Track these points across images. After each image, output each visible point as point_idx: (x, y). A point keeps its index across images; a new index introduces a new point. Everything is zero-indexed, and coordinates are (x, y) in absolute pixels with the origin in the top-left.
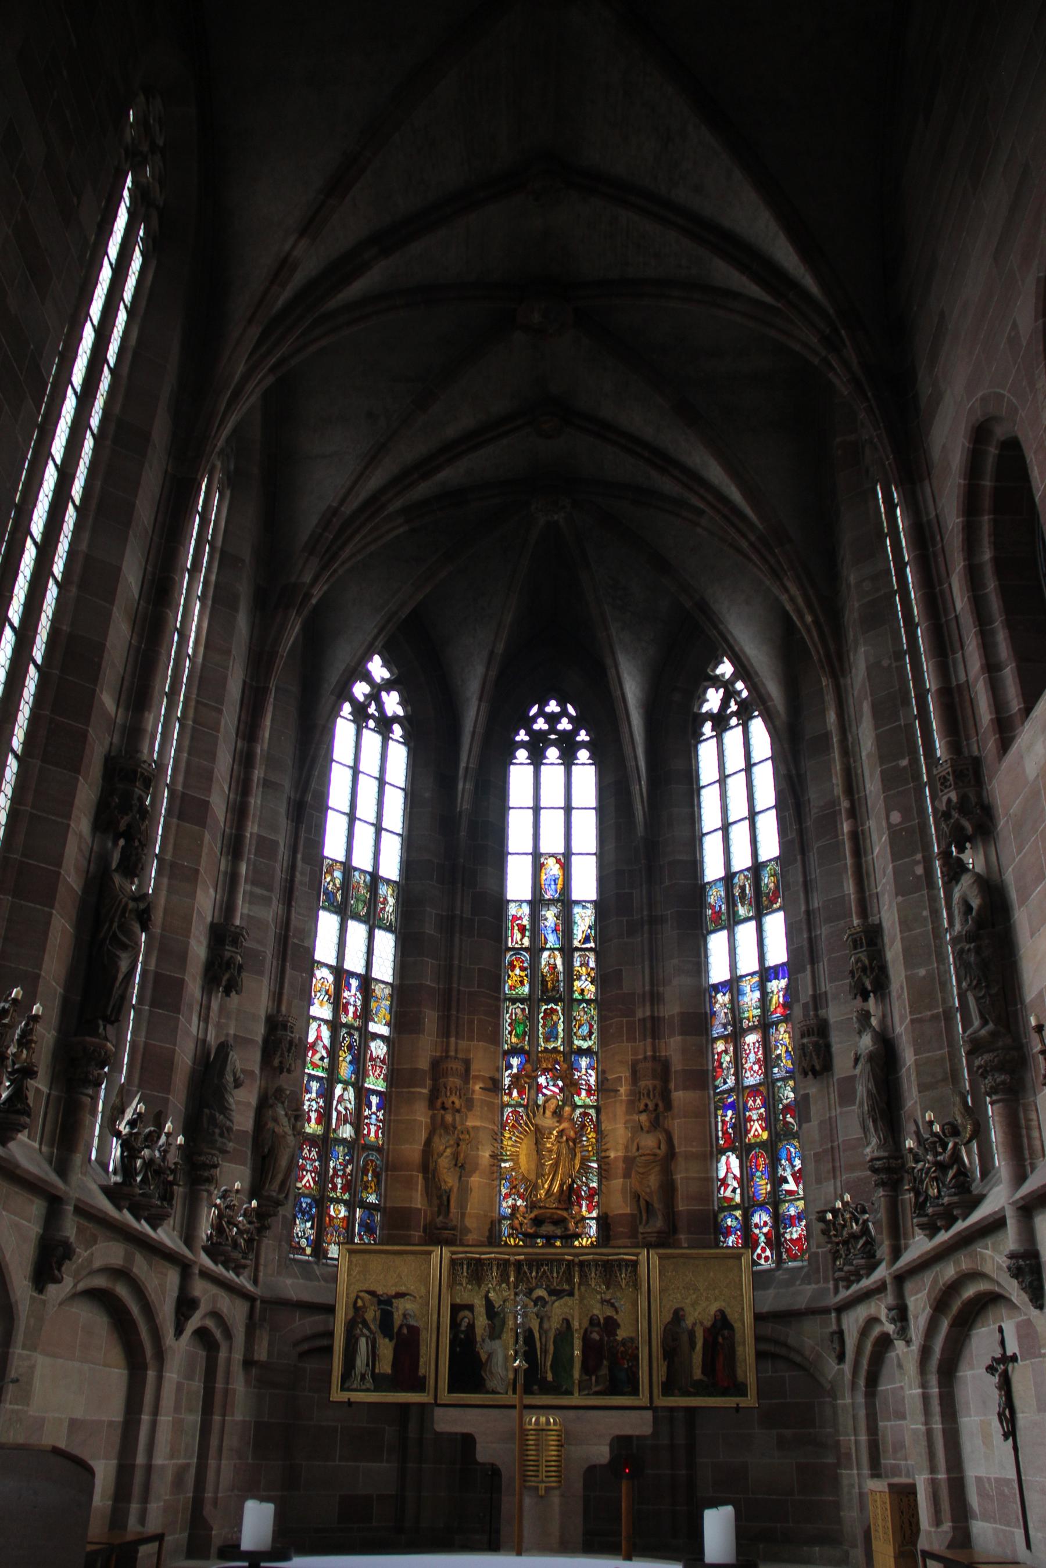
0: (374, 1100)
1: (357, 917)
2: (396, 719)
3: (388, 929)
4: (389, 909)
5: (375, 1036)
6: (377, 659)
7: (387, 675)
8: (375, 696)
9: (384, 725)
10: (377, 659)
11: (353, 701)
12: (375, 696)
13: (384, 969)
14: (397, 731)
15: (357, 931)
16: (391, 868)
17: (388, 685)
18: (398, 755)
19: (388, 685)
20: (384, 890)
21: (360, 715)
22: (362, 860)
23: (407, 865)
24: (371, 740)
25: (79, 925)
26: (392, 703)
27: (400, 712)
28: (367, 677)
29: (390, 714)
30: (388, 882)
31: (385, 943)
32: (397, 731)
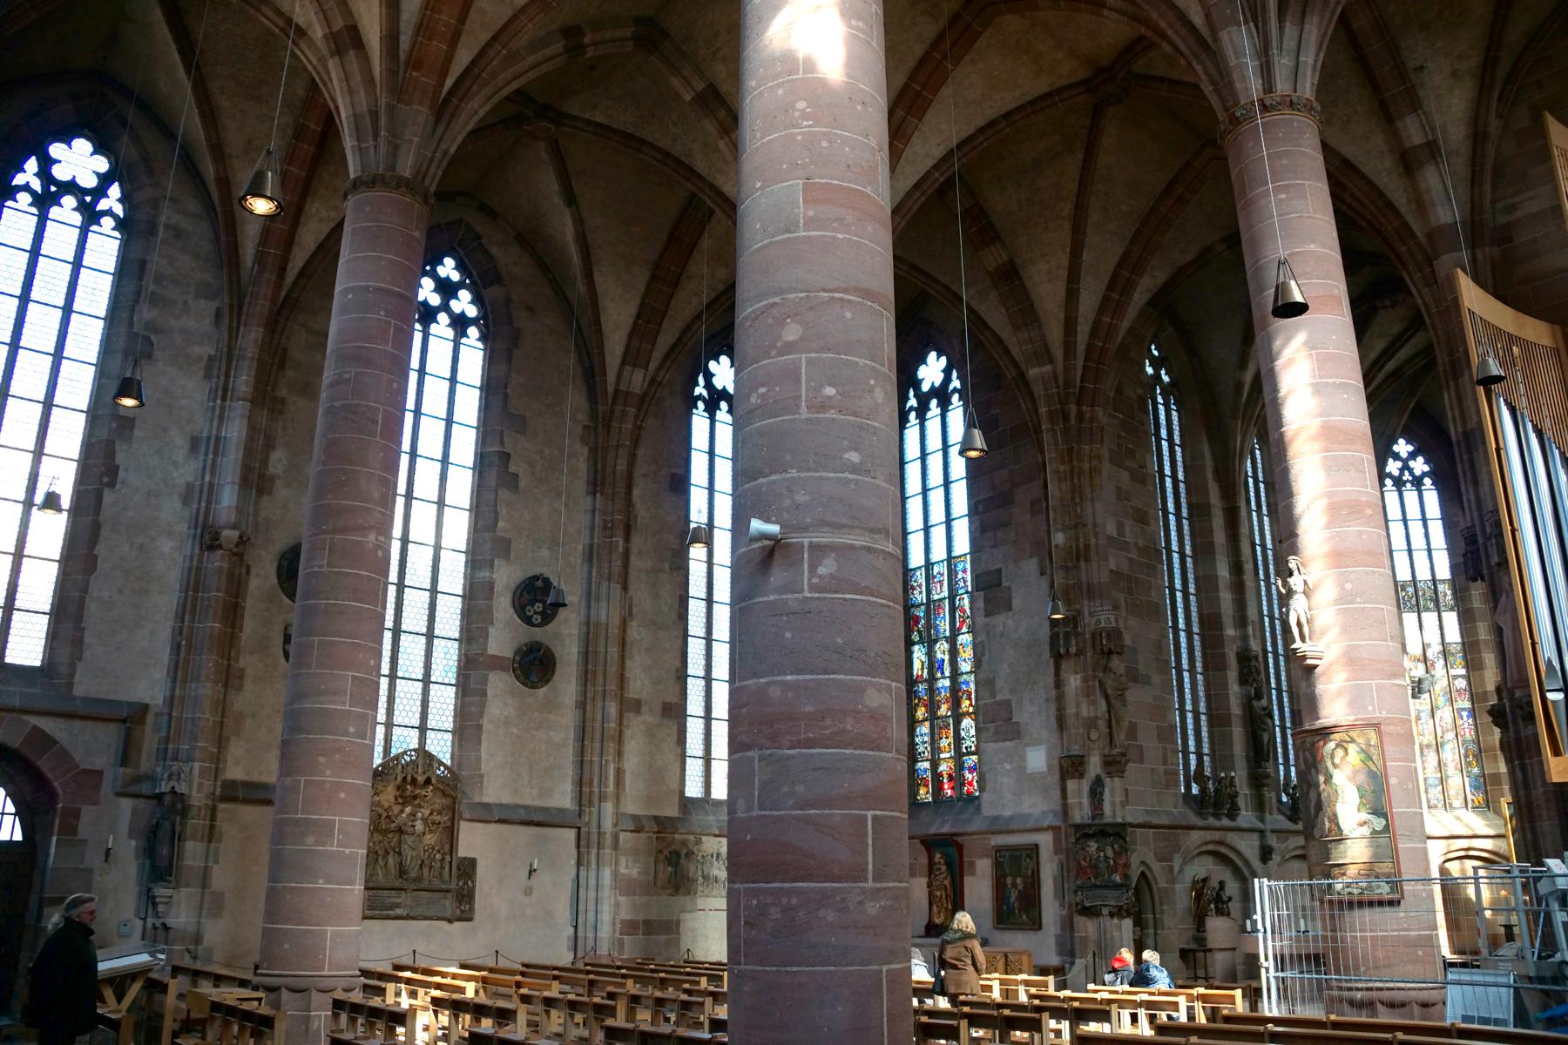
0: (1465, 714)
1: (1427, 609)
2: (1424, 474)
3: (1452, 609)
4: (1449, 597)
5: (1455, 677)
6: (1402, 441)
7: (1410, 448)
8: (1406, 467)
9: (1417, 482)
10: (1402, 441)
11: (1390, 476)
12: (1406, 467)
13: (1454, 634)
14: (1427, 481)
15: (1430, 618)
16: (1444, 572)
17: (1412, 456)
18: (1432, 498)
19: (1412, 456)
20: (1441, 587)
21: (1399, 483)
22: (1423, 574)
23: (1454, 568)
24: (1411, 496)
25: (1245, 726)
26: (1419, 466)
27: (1426, 468)
28: (1396, 457)
29: (1418, 472)
30: (1444, 581)
31: (1451, 619)
32: (1427, 481)
